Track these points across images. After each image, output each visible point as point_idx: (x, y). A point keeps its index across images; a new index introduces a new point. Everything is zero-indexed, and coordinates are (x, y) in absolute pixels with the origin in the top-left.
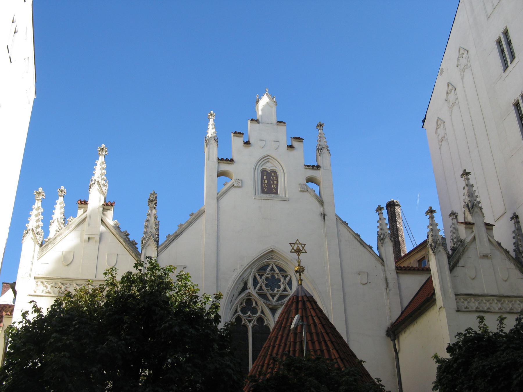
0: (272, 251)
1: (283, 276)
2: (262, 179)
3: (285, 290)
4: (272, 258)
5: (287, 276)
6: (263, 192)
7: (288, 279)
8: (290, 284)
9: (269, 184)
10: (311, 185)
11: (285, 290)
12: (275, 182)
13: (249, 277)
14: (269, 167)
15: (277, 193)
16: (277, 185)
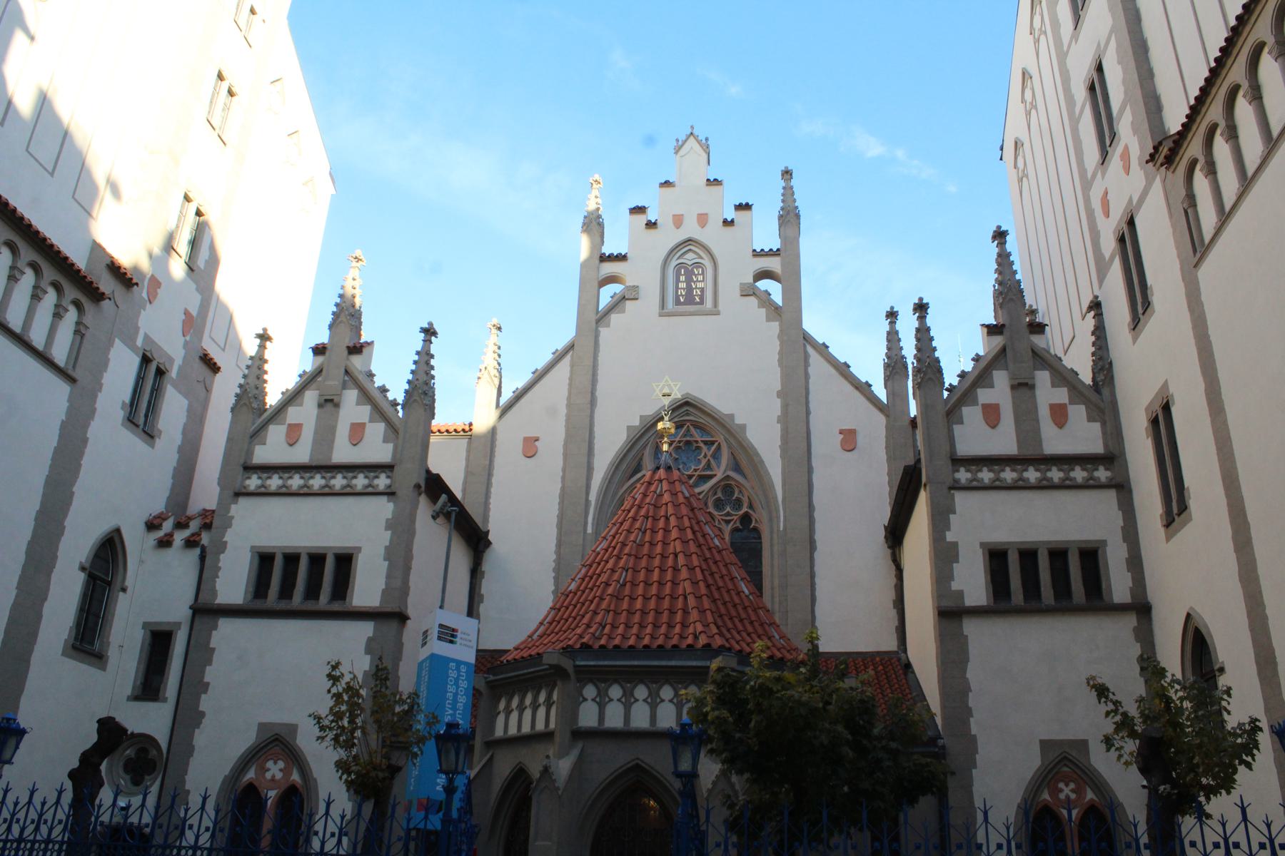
0: (687, 403)
1: (705, 443)
2: (678, 281)
3: (708, 466)
4: (688, 414)
5: (712, 443)
6: (678, 302)
7: (713, 448)
8: (717, 455)
9: (689, 290)
10: (764, 284)
11: (708, 466)
12: (700, 285)
13: (644, 447)
14: (690, 258)
15: (702, 302)
16: (702, 290)
